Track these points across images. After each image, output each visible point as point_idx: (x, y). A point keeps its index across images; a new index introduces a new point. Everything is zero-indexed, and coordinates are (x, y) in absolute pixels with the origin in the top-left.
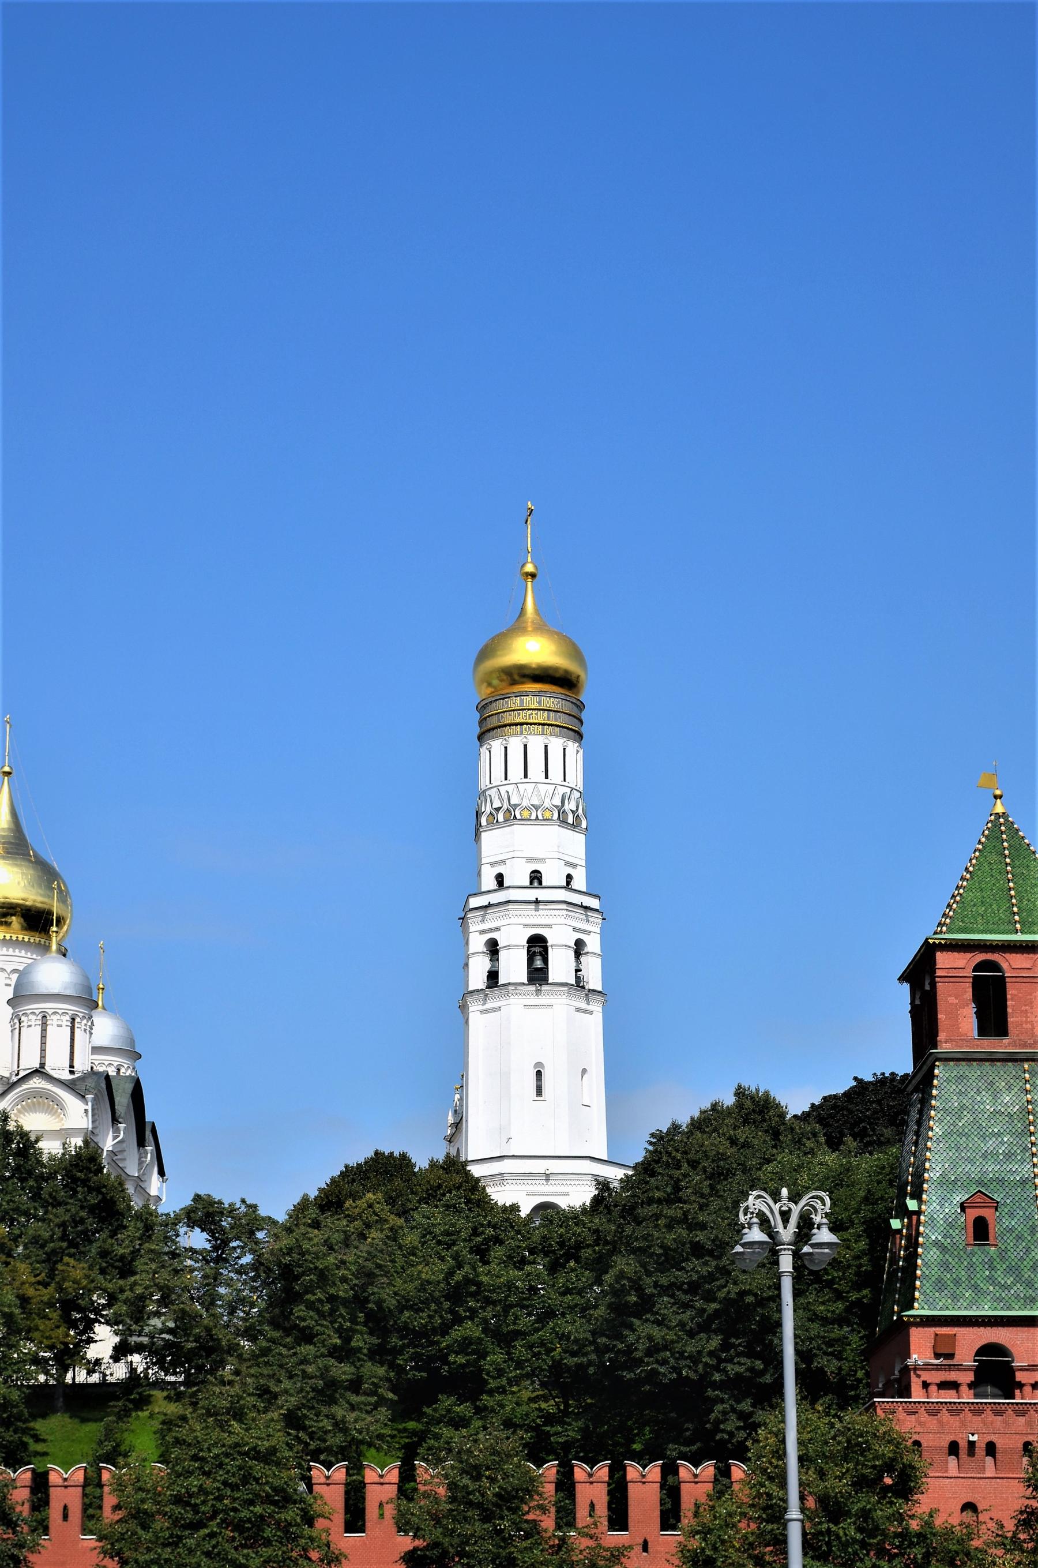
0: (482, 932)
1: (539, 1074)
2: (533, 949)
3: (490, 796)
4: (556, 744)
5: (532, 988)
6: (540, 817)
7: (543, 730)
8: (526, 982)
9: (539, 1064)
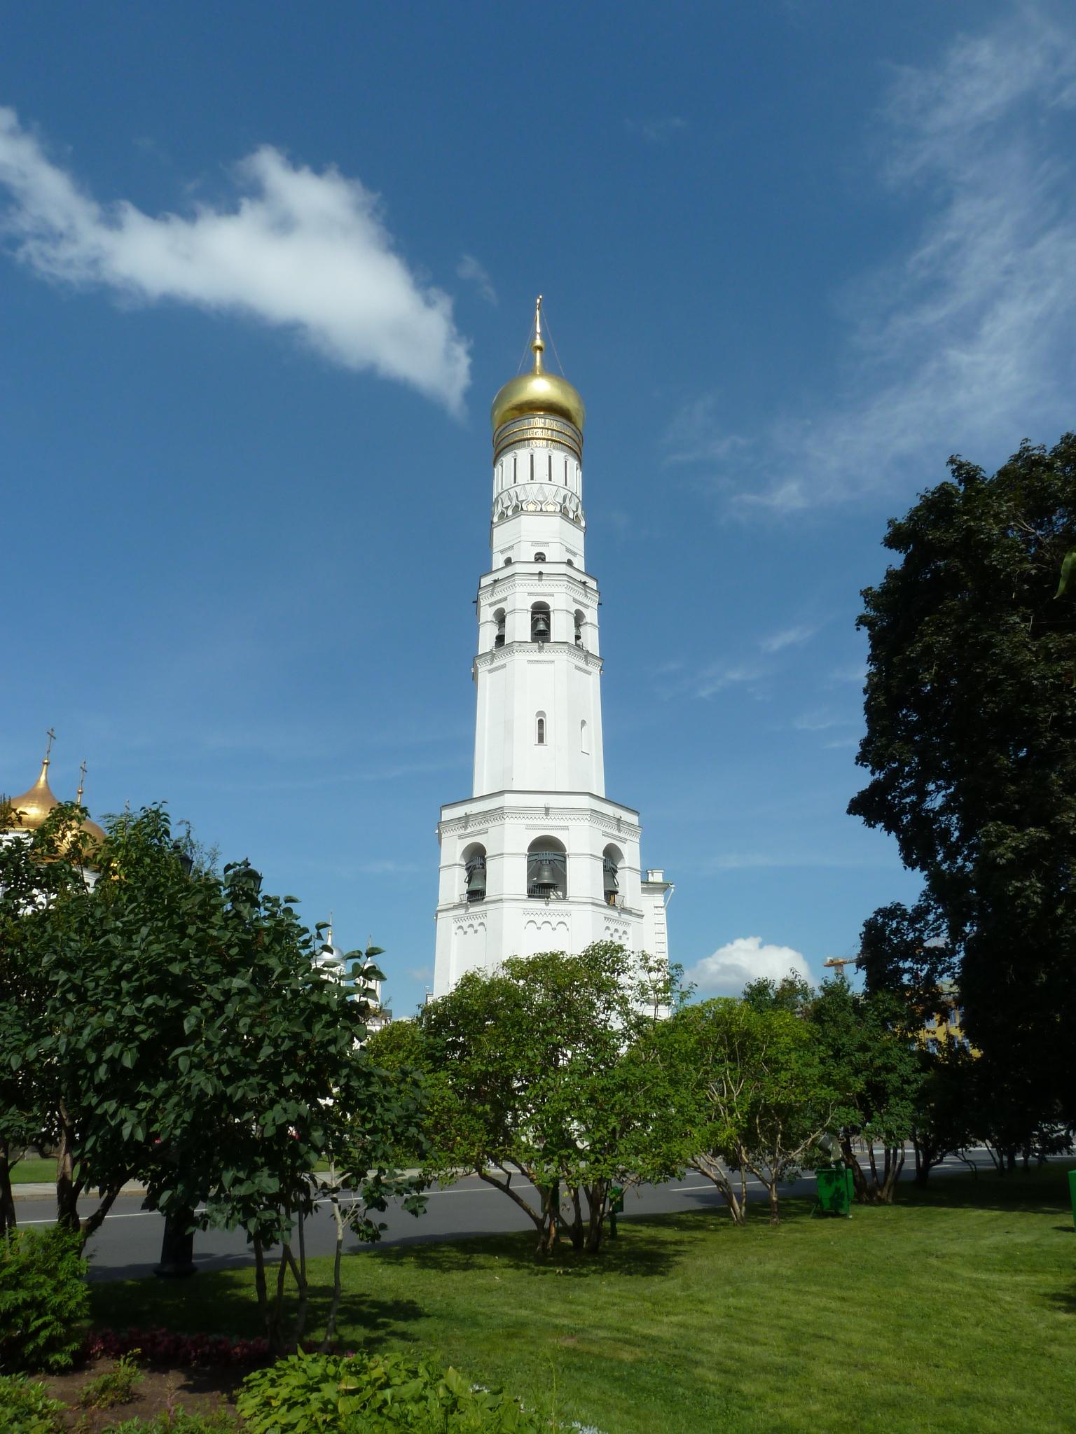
0: (491, 605)
1: (541, 722)
2: (537, 616)
4: (559, 456)
5: (535, 645)
6: (544, 510)
7: (547, 444)
9: (541, 713)
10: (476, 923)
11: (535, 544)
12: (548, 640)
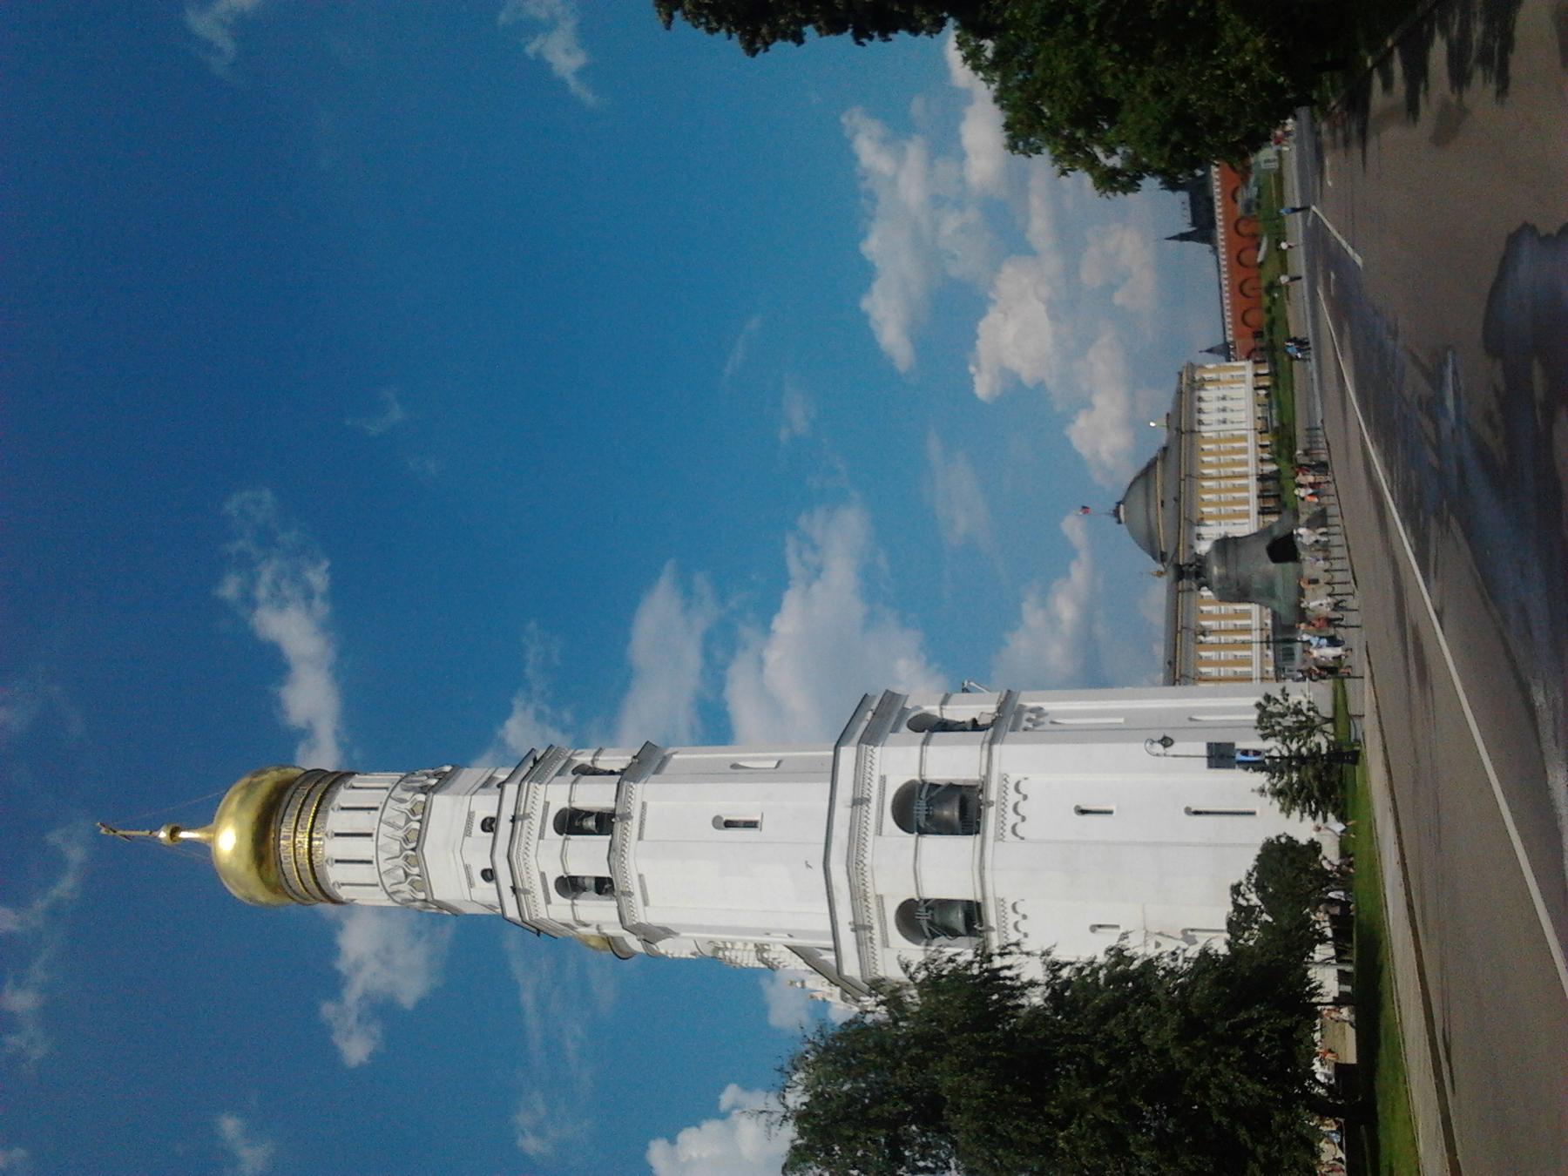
0: (548, 902)
1: (729, 824)
3: (392, 885)
5: (618, 827)
6: (419, 817)
8: (609, 837)
10: (1012, 918)
11: (468, 832)
12: (612, 814)
